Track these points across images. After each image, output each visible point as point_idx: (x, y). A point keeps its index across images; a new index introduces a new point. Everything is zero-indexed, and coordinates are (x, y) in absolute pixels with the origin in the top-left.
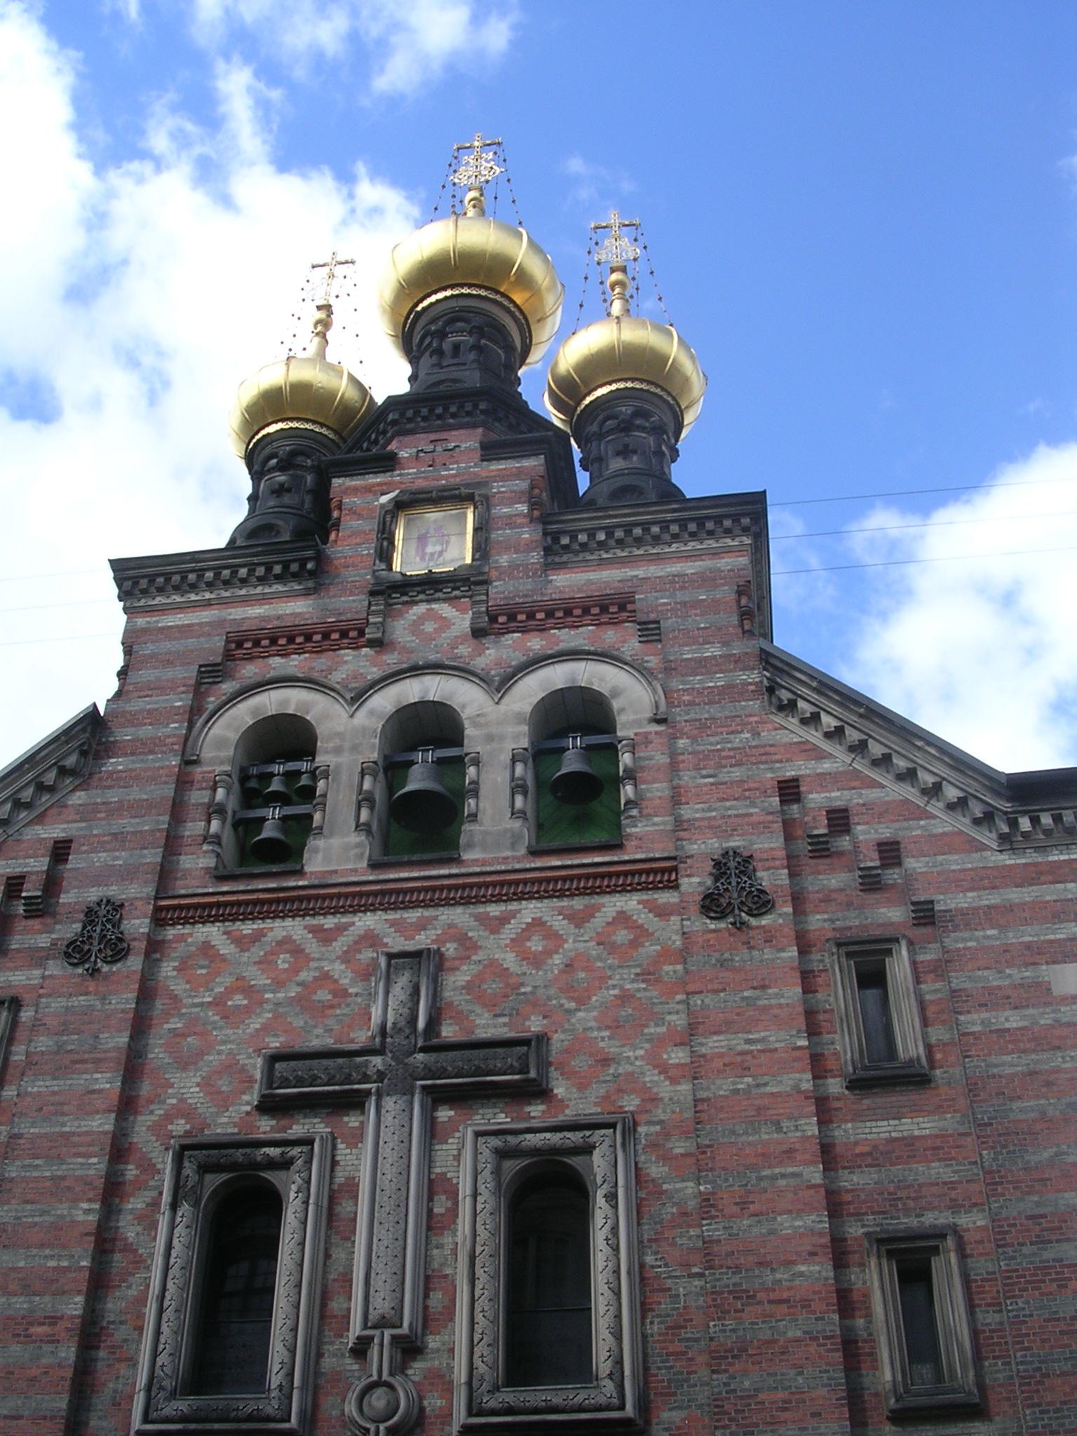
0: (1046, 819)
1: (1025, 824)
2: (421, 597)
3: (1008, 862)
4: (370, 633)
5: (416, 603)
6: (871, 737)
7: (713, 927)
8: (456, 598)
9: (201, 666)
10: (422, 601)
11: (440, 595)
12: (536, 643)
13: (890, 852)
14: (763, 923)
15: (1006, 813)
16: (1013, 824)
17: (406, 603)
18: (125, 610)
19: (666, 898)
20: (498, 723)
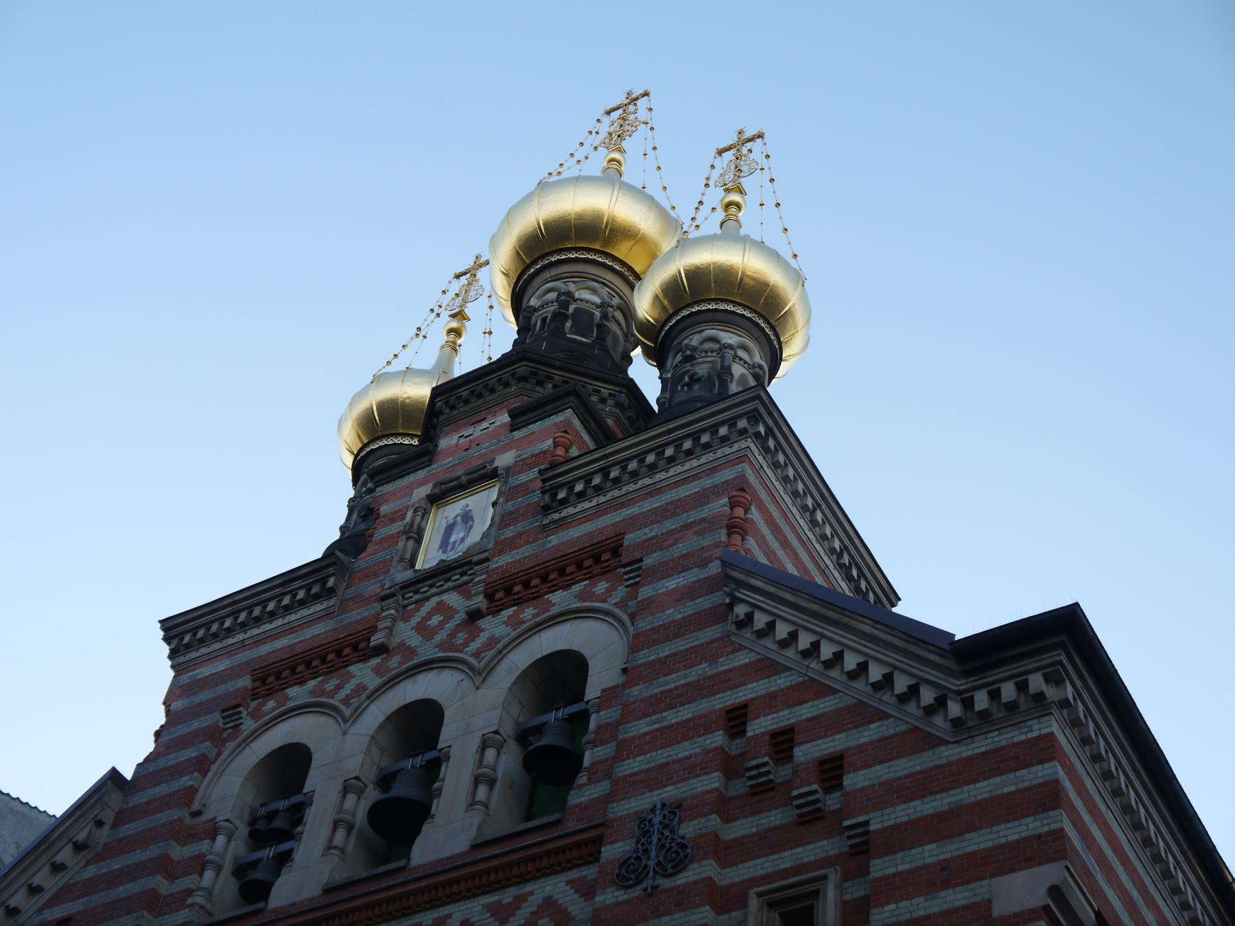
0: (1008, 691)
1: (981, 701)
2: (434, 590)
3: (964, 755)
4: (377, 639)
5: (428, 599)
6: (823, 636)
7: (626, 897)
8: (465, 583)
9: (223, 711)
10: (433, 595)
11: (450, 584)
12: (528, 613)
13: (831, 770)
14: (679, 882)
15: (959, 693)
16: (968, 704)
17: (416, 602)
18: (173, 667)
19: (590, 872)
20: (478, 712)
